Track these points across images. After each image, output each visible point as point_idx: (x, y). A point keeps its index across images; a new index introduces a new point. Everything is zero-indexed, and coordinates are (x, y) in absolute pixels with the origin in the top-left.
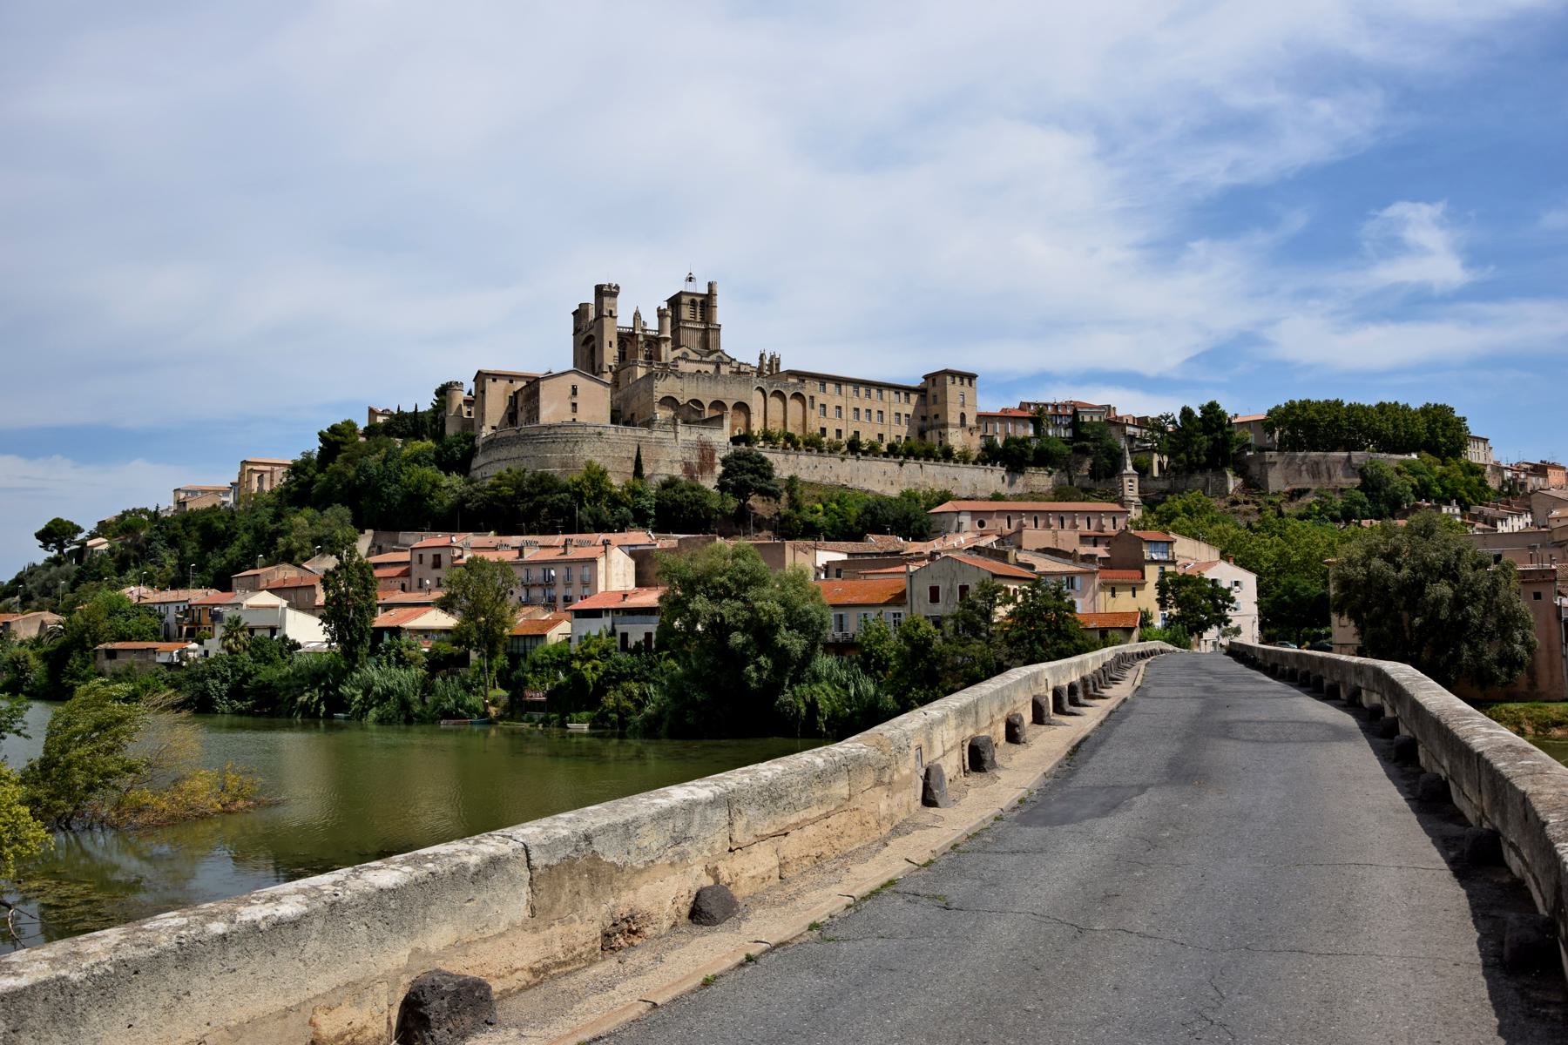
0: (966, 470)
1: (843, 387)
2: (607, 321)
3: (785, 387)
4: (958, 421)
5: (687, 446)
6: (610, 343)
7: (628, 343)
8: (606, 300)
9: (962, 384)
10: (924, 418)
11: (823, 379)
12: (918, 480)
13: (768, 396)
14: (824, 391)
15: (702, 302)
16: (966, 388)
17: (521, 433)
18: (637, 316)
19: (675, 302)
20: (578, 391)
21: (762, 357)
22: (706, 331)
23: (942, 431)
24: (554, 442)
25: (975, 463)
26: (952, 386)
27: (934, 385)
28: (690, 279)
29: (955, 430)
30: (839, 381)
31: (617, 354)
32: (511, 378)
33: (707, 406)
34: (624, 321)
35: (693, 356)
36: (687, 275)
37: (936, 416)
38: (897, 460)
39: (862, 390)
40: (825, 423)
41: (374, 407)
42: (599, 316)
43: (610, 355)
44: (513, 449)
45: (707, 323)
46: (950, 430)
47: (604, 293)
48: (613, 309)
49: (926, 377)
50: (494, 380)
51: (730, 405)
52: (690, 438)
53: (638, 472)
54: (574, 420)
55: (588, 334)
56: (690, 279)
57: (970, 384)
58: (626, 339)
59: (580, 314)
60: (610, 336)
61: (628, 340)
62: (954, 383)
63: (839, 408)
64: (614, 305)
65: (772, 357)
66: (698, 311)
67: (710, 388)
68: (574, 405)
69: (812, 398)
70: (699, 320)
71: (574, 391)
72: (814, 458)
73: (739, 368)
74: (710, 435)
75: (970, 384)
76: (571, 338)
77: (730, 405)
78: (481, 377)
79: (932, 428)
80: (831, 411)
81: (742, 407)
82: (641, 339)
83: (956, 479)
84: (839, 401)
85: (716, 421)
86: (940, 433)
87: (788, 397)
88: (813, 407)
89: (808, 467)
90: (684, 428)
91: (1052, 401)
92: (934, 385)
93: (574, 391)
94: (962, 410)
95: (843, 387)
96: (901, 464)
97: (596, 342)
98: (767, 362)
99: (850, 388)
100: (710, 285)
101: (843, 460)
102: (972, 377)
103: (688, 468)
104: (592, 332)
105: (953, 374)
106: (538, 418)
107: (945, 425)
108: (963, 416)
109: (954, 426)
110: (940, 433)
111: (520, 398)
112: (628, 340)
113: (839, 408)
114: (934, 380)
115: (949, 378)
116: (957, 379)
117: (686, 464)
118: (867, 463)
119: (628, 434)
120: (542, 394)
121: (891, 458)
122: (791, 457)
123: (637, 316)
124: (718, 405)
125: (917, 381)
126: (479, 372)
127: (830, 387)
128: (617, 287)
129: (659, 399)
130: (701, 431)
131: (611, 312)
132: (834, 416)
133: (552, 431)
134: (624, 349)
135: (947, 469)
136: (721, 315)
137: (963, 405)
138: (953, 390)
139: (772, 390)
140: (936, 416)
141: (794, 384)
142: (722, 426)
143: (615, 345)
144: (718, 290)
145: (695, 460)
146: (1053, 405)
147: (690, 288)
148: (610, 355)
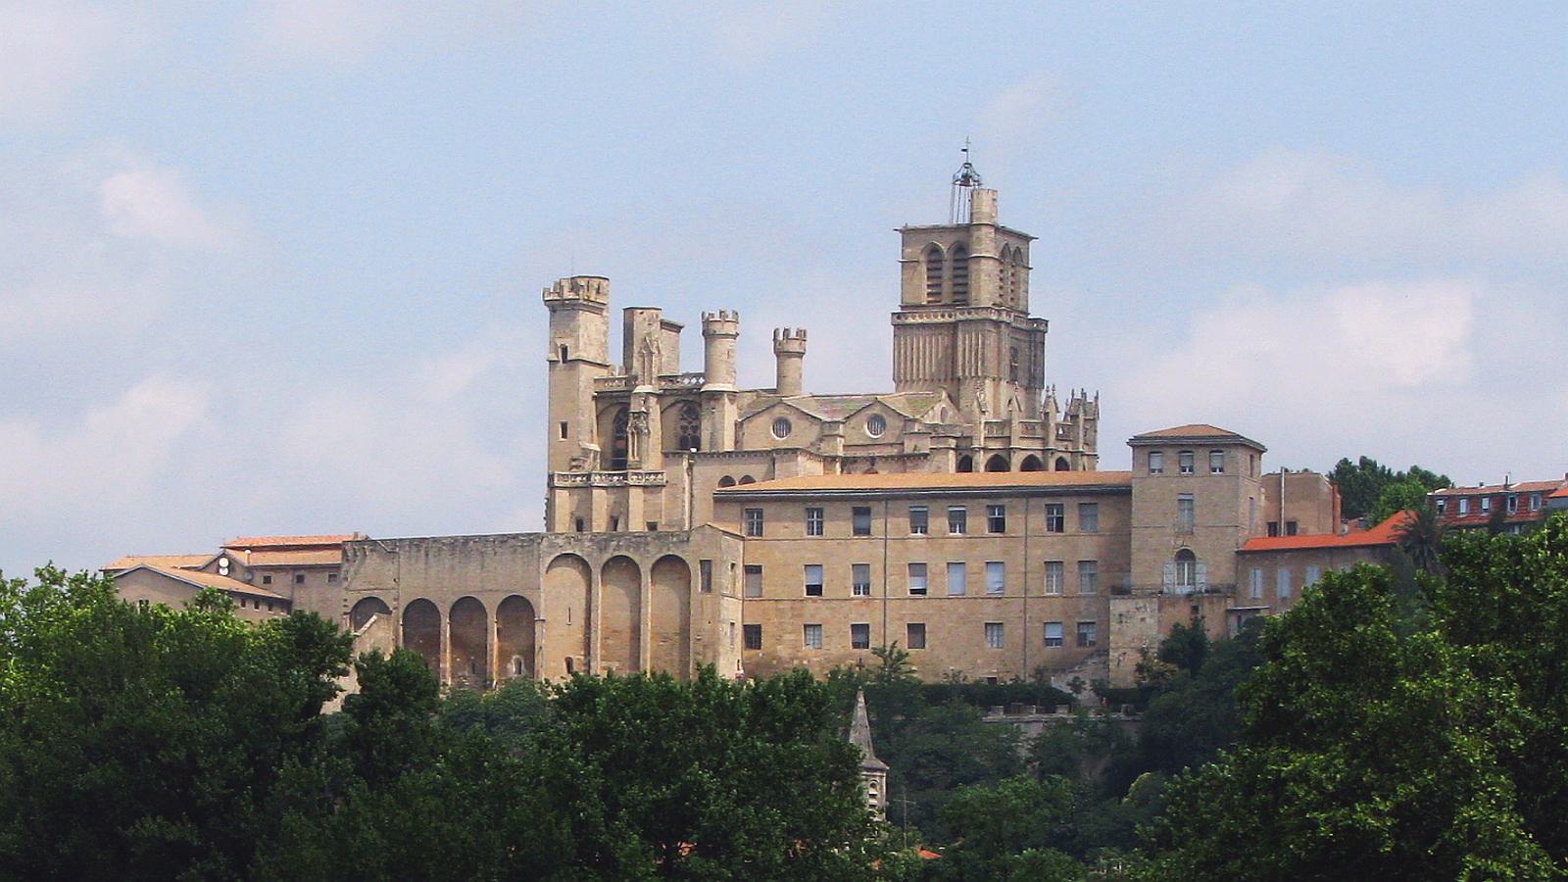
3: (637, 549)
6: (564, 426)
13: (597, 576)
33: (445, 611)
48: (568, 343)
51: (491, 604)
56: (966, 180)
63: (861, 569)
64: (573, 333)
66: (947, 273)
67: (452, 568)
69: (706, 565)
77: (491, 604)
81: (519, 610)
84: (862, 550)
88: (708, 587)
139: (607, 556)
146: (1492, 497)
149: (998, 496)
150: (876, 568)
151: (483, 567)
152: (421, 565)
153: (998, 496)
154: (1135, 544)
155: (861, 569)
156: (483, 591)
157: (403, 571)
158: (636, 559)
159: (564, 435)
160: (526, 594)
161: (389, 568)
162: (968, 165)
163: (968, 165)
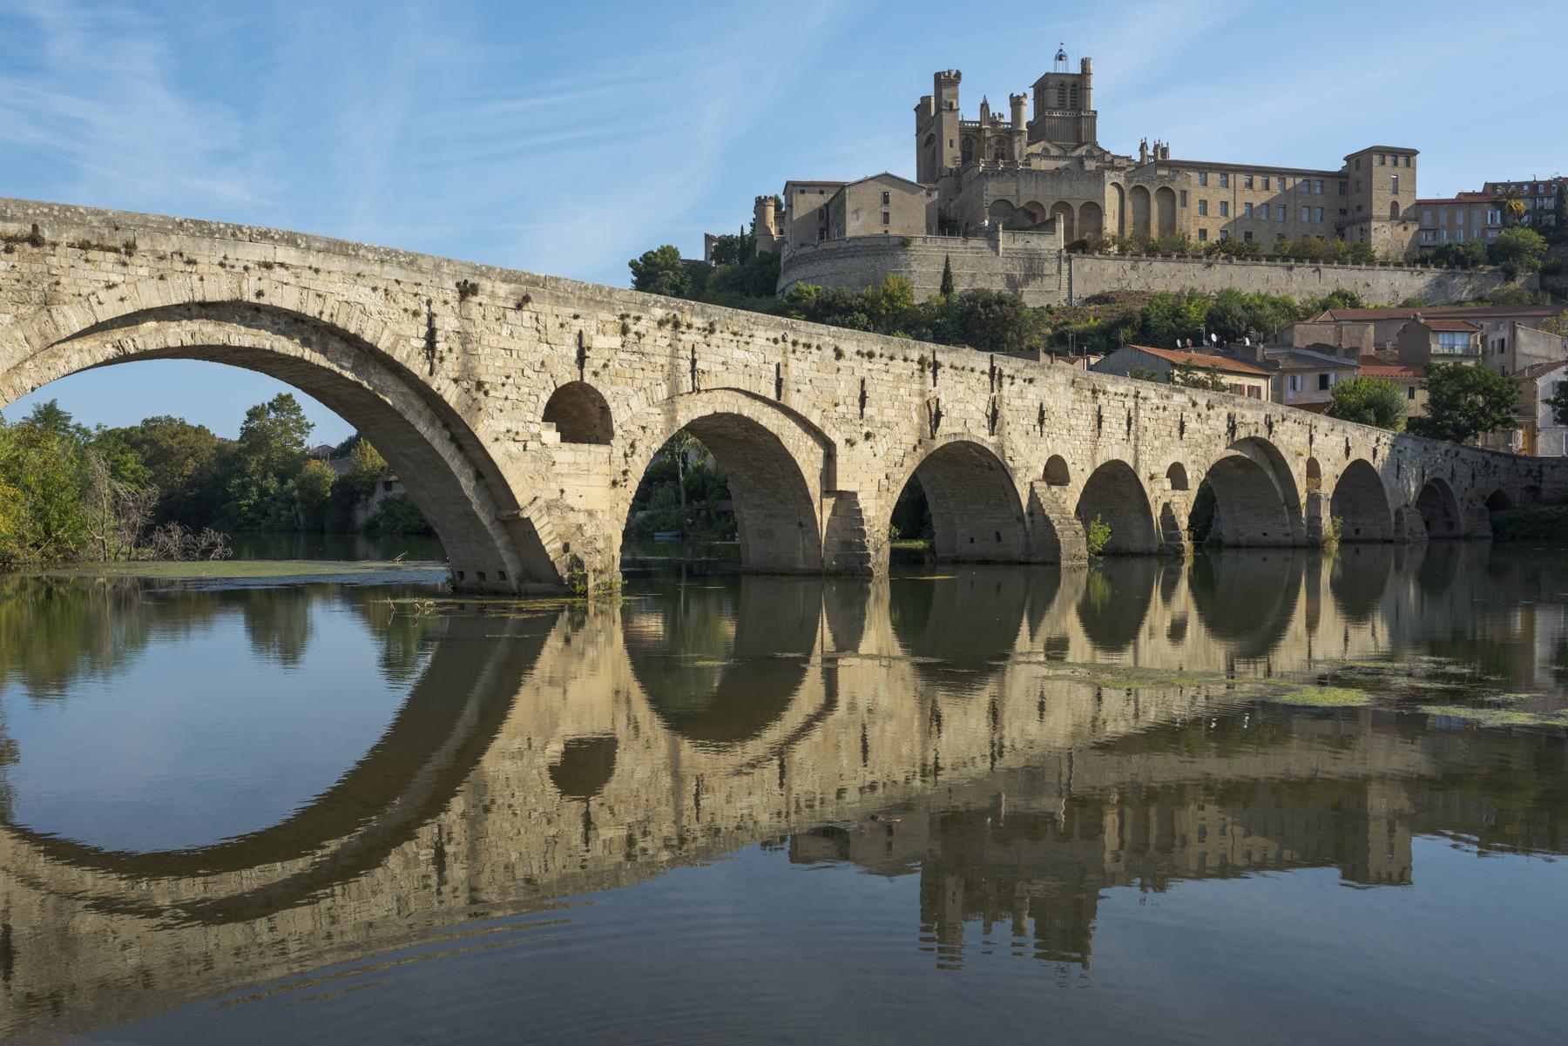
0: (1384, 274)
1: (1231, 176)
2: (946, 116)
3: (1148, 182)
4: (1387, 212)
5: (1011, 255)
6: (951, 142)
7: (974, 141)
8: (945, 91)
9: (1396, 163)
10: (1343, 212)
11: (1204, 168)
12: (1312, 288)
13: (1127, 194)
14: (1205, 184)
15: (1074, 85)
16: (1401, 169)
17: (819, 248)
18: (985, 106)
19: (1041, 87)
20: (891, 199)
21: (1142, 149)
22: (1078, 119)
23: (1364, 226)
24: (853, 256)
25: (1398, 265)
26: (1381, 168)
27: (1358, 168)
28: (1061, 59)
29: (1380, 224)
30: (1225, 170)
31: (959, 154)
32: (821, 187)
34: (969, 112)
35: (1054, 152)
36: (1055, 52)
37: (1359, 208)
38: (1286, 264)
39: (1258, 180)
40: (1205, 223)
41: (711, 233)
42: (939, 110)
43: (950, 156)
44: (811, 267)
45: (1080, 110)
46: (1374, 225)
47: (946, 82)
49: (1348, 159)
50: (803, 192)
52: (1013, 246)
53: (946, 288)
54: (886, 232)
55: (929, 133)
56: (1060, 57)
57: (1408, 165)
58: (971, 137)
59: (922, 109)
60: (950, 133)
61: (975, 138)
62: (1383, 163)
63: (1226, 203)
64: (956, 96)
65: (1156, 147)
68: (886, 215)
69: (1184, 193)
70: (1069, 107)
71: (886, 199)
72: (1172, 264)
73: (1112, 162)
74: (1040, 242)
75: (1408, 165)
76: (914, 139)
78: (791, 187)
79: (1354, 222)
80: (1214, 208)
82: (988, 134)
83: (1368, 285)
84: (1225, 195)
85: (1047, 226)
86: (1362, 229)
87: (1152, 192)
88: (1184, 204)
89: (1164, 276)
90: (1006, 235)
91: (1531, 179)
92: (1358, 168)
93: (886, 199)
94: (1394, 198)
95: (1231, 176)
96: (1290, 268)
97: (936, 143)
98: (1150, 152)
99: (1242, 179)
100: (1085, 63)
101: (1210, 265)
102: (1410, 154)
103: (1011, 281)
104: (933, 131)
105: (1382, 151)
106: (844, 231)
107: (1369, 218)
108: (1395, 206)
109: (1380, 219)
110: (1362, 229)
111: (831, 210)
112: (975, 138)
113: (1226, 203)
114: (1358, 161)
115: (1376, 159)
116: (1389, 159)
117: (1008, 276)
118: (1244, 269)
119: (939, 244)
120: (849, 206)
121: (1279, 262)
122: (1142, 265)
123: (985, 106)
124: (1063, 206)
125: (1336, 164)
126: (787, 183)
127: (1214, 178)
128: (958, 75)
129: (990, 204)
130: (1028, 237)
131: (951, 104)
132: (1218, 215)
133: (850, 244)
134: (970, 147)
135: (1355, 273)
136: (1095, 101)
137: (1395, 192)
138: (1382, 175)
139: (1132, 185)
140: (1359, 208)
141: (1161, 177)
142: (1054, 231)
143: (957, 144)
144: (1093, 67)
145: (1018, 273)
147: (1061, 68)
148: (950, 156)
149: (1284, 173)
150: (1231, 204)
151: (1070, 187)
152: (1033, 184)
153: (1284, 173)
154: (1374, 198)
155: (1225, 204)
156: (1070, 199)
157: (1022, 186)
158: (1148, 188)
159: (951, 146)
160: (1098, 202)
161: (1012, 186)
162: (1061, 50)
163: (1061, 50)
